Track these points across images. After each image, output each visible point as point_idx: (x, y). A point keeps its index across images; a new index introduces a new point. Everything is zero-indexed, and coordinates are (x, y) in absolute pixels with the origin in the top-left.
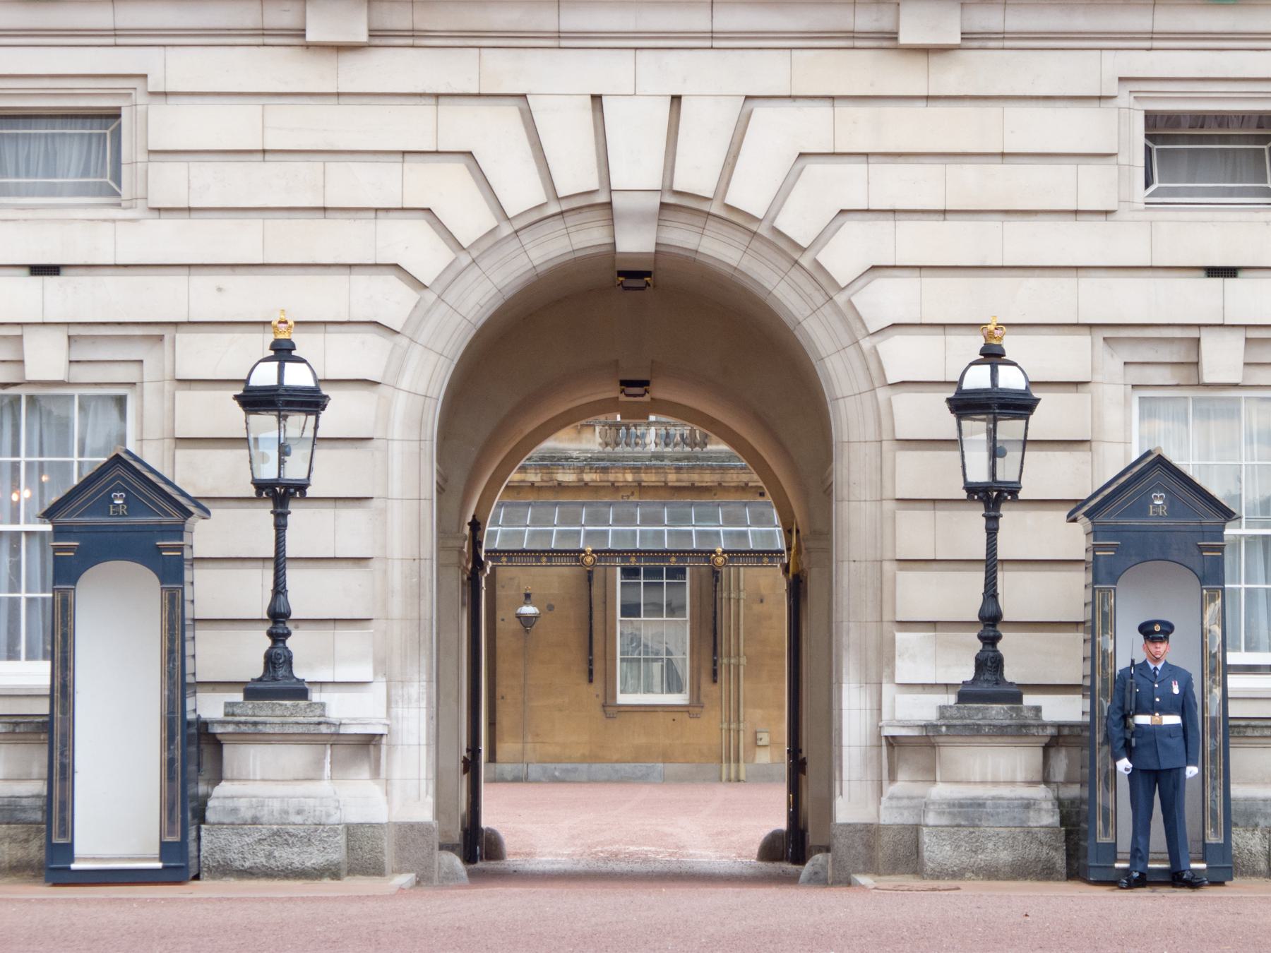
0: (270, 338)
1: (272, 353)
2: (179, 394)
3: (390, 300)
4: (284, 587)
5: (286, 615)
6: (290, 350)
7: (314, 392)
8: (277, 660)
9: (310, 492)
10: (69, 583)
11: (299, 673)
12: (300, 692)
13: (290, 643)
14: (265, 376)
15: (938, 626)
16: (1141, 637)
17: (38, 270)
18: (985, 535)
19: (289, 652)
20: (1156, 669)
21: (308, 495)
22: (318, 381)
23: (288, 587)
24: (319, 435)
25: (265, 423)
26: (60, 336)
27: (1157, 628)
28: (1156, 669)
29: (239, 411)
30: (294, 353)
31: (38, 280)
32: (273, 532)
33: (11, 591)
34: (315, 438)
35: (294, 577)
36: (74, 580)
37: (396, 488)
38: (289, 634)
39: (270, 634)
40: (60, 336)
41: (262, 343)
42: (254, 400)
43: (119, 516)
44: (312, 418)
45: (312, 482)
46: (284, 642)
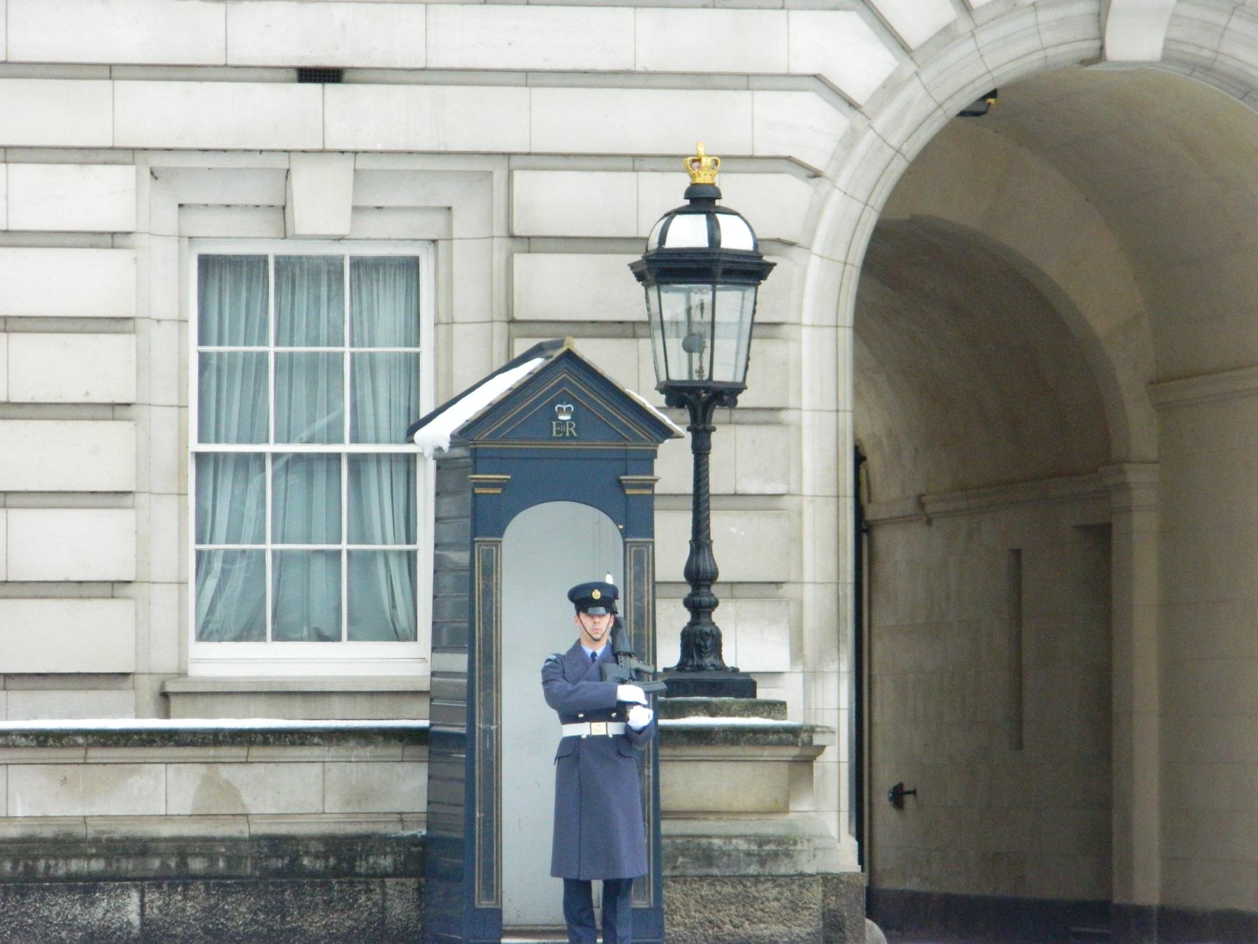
0: (684, 182)
1: (687, 202)
2: (520, 260)
3: (806, 126)
4: (708, 536)
5: (712, 577)
6: (712, 200)
7: (755, 255)
8: (700, 641)
9: (743, 400)
10: (493, 535)
11: (729, 659)
12: (742, 687)
13: (717, 616)
14: (689, 233)
15: (738, 591)
16: (572, 605)
17: (309, 75)
18: (692, 456)
19: (717, 628)
20: (594, 654)
21: (740, 405)
22: (757, 243)
23: (712, 537)
24: (758, 318)
25: (674, 302)
26: (341, 171)
27: (597, 595)
28: (594, 654)
29: (639, 287)
30: (717, 203)
31: (313, 89)
32: (690, 458)
33: (408, 542)
34: (753, 324)
35: (721, 525)
36: (499, 530)
37: (807, 400)
38: (715, 605)
39: (689, 603)
40: (341, 171)
41: (674, 188)
42: (664, 268)
43: (564, 438)
44: (750, 293)
45: (748, 383)
46: (710, 614)
